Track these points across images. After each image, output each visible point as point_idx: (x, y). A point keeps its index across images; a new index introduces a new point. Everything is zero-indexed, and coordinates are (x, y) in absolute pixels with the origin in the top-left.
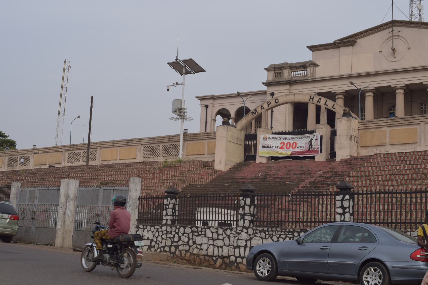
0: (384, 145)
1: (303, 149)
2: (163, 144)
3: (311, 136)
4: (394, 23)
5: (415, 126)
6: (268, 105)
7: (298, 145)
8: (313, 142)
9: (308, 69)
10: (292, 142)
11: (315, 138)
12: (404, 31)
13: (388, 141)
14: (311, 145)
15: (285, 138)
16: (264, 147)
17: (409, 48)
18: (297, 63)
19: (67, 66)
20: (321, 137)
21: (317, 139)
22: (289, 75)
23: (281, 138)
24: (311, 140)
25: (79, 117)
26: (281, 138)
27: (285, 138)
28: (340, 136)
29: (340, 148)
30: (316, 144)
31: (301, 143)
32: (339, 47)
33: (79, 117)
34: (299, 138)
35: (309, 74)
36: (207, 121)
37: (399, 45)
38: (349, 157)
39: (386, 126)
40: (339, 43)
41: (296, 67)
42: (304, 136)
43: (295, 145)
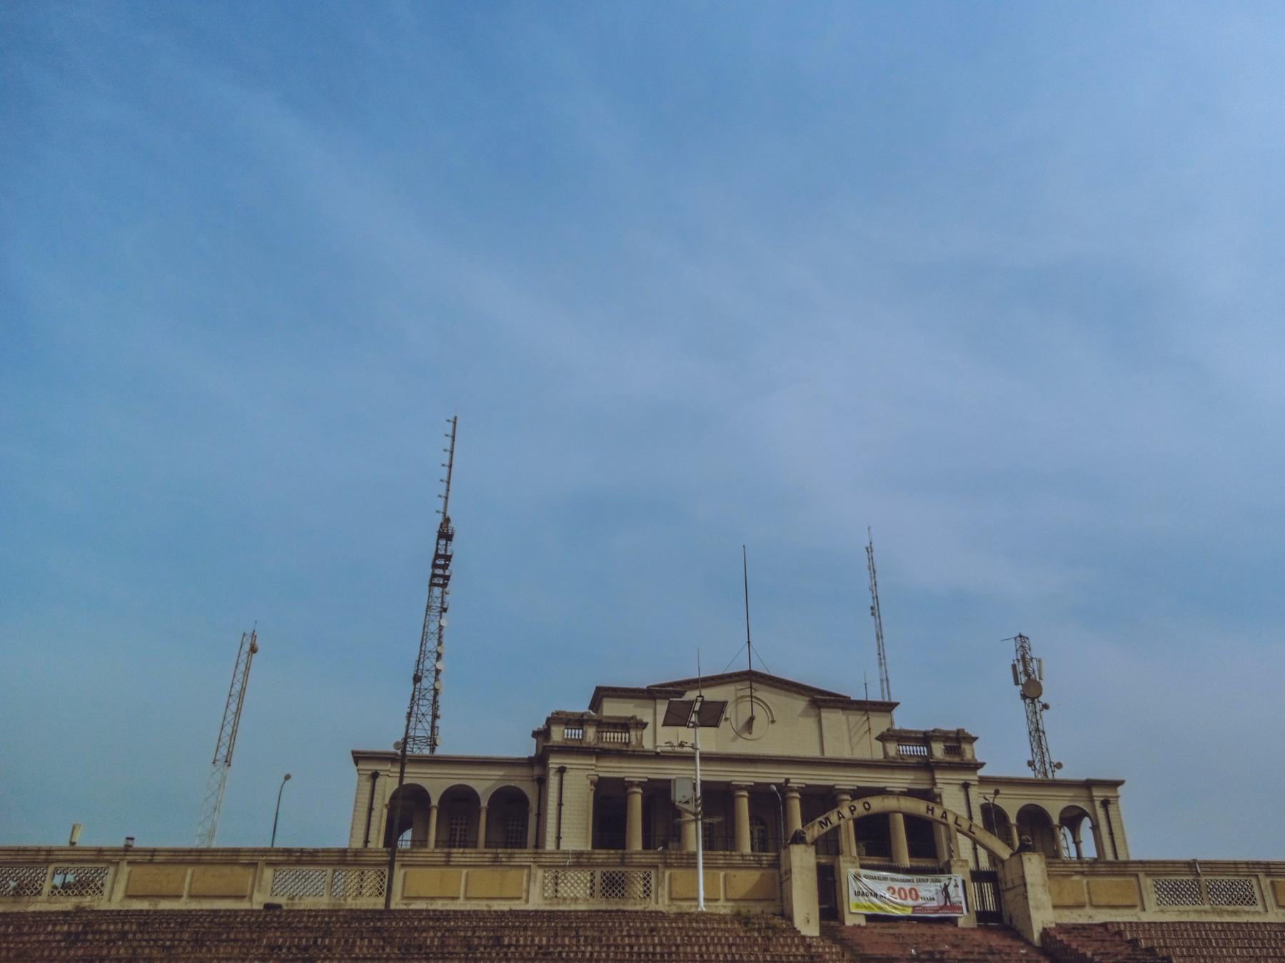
0: (1081, 906)
1: (935, 904)
2: (605, 870)
3: (944, 878)
4: (751, 677)
5: (1128, 879)
6: (852, 812)
7: (921, 894)
8: (951, 889)
9: (633, 733)
10: (907, 886)
11: (953, 882)
12: (763, 693)
13: (1086, 898)
14: (947, 896)
15: (892, 880)
16: (858, 894)
17: (773, 722)
18: (613, 718)
19: (247, 647)
20: (964, 882)
21: (956, 886)
22: (600, 739)
23: (885, 879)
24: (946, 887)
25: (287, 777)
26: (885, 879)
27: (892, 880)
28: (1032, 885)
29: (1037, 908)
30: (957, 895)
31: (928, 891)
32: (655, 699)
33: (287, 777)
34: (919, 881)
35: (634, 742)
36: (375, 806)
37: (759, 712)
38: (1053, 925)
39: (1082, 873)
40: (658, 692)
41: (609, 724)
42: (930, 877)
43: (914, 894)
